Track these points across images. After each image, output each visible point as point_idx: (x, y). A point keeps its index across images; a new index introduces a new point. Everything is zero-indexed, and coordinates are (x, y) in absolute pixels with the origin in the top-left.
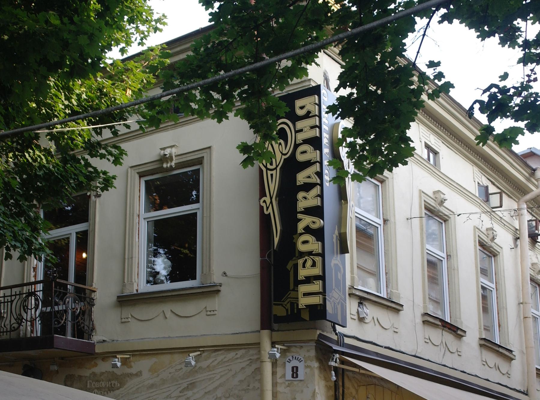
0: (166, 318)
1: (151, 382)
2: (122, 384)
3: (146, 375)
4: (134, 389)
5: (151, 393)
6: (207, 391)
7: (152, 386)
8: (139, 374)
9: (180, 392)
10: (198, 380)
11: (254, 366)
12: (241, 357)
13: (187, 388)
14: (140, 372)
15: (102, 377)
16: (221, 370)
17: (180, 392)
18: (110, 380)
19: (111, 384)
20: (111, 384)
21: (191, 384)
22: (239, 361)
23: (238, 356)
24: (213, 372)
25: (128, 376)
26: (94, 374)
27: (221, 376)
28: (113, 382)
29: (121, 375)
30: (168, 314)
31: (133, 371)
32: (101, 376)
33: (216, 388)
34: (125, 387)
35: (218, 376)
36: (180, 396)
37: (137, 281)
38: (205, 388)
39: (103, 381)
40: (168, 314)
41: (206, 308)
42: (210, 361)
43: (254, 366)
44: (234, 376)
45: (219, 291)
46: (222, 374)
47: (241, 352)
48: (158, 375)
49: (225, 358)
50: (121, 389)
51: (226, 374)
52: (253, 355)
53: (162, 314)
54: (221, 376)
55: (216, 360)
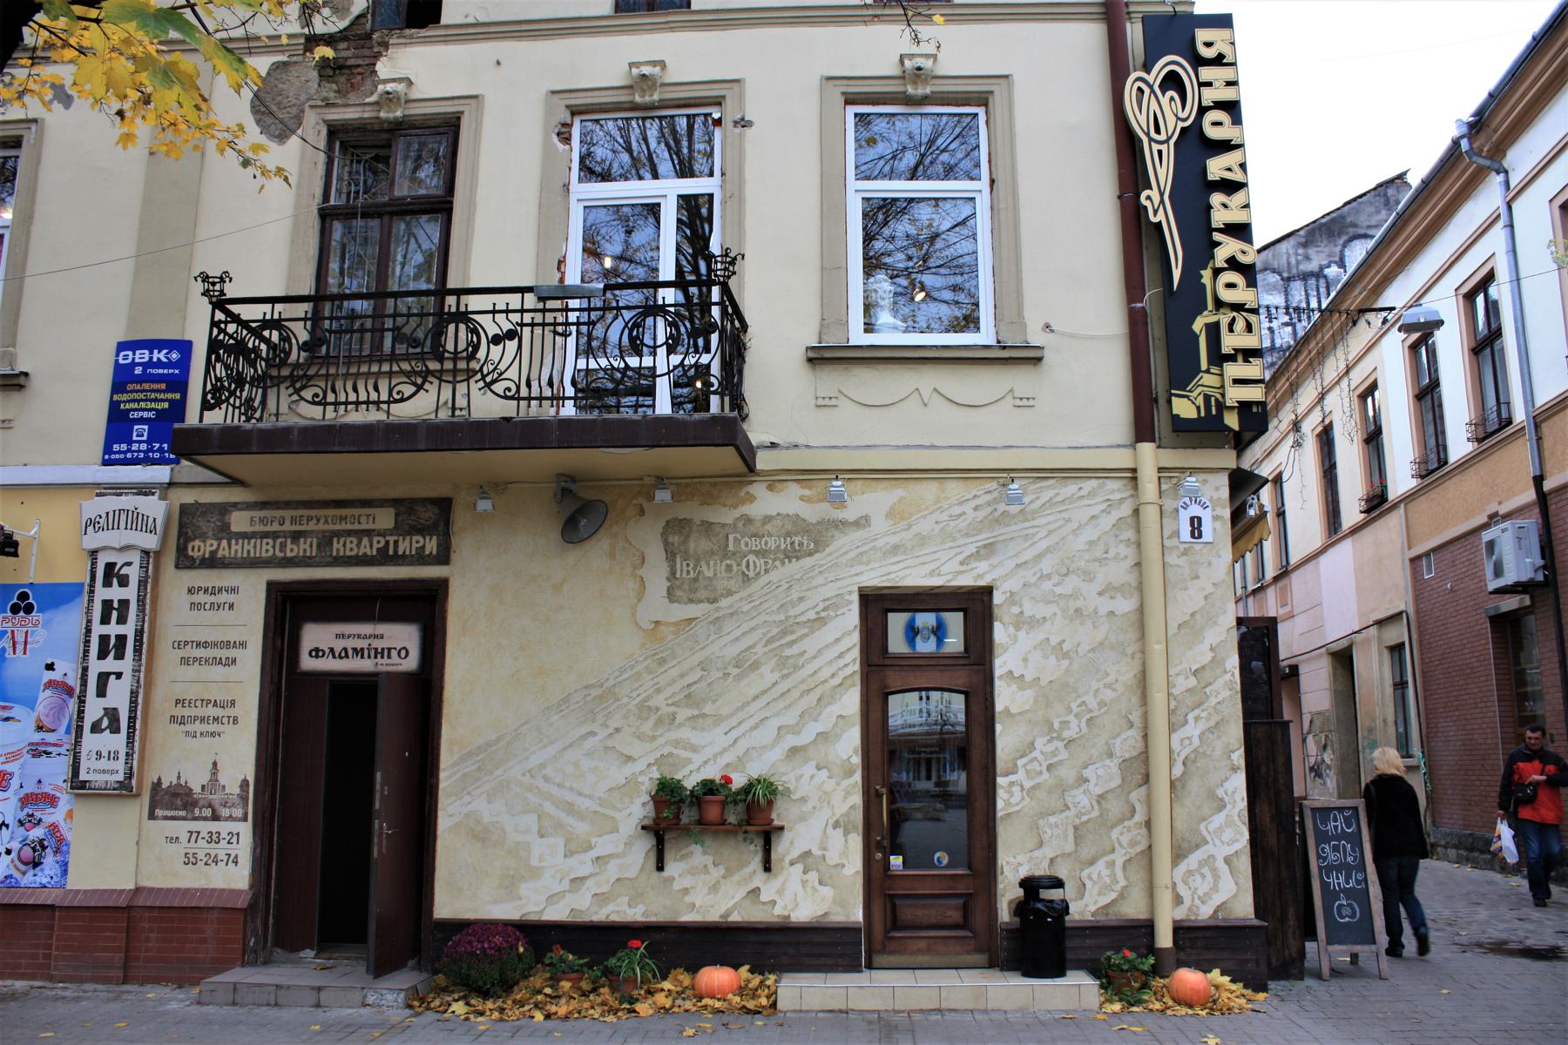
1: (893, 540)
2: (819, 545)
3: (879, 524)
4: (852, 555)
5: (893, 564)
7: (895, 549)
9: (962, 563)
12: (1091, 494)
13: (977, 556)
15: (768, 527)
17: (962, 563)
18: (788, 534)
19: (792, 543)
20: (792, 543)
21: (985, 546)
22: (1086, 502)
25: (837, 527)
26: (748, 520)
27: (1050, 532)
28: (797, 539)
29: (819, 523)
31: (850, 514)
33: (1040, 556)
34: (828, 550)
35: (1043, 533)
38: (1016, 555)
39: (770, 535)
41: (1011, 390)
45: (1039, 359)
46: (1051, 527)
48: (910, 526)
49: (1057, 494)
50: (817, 555)
51: (1060, 527)
52: (1113, 491)
55: (1038, 498)
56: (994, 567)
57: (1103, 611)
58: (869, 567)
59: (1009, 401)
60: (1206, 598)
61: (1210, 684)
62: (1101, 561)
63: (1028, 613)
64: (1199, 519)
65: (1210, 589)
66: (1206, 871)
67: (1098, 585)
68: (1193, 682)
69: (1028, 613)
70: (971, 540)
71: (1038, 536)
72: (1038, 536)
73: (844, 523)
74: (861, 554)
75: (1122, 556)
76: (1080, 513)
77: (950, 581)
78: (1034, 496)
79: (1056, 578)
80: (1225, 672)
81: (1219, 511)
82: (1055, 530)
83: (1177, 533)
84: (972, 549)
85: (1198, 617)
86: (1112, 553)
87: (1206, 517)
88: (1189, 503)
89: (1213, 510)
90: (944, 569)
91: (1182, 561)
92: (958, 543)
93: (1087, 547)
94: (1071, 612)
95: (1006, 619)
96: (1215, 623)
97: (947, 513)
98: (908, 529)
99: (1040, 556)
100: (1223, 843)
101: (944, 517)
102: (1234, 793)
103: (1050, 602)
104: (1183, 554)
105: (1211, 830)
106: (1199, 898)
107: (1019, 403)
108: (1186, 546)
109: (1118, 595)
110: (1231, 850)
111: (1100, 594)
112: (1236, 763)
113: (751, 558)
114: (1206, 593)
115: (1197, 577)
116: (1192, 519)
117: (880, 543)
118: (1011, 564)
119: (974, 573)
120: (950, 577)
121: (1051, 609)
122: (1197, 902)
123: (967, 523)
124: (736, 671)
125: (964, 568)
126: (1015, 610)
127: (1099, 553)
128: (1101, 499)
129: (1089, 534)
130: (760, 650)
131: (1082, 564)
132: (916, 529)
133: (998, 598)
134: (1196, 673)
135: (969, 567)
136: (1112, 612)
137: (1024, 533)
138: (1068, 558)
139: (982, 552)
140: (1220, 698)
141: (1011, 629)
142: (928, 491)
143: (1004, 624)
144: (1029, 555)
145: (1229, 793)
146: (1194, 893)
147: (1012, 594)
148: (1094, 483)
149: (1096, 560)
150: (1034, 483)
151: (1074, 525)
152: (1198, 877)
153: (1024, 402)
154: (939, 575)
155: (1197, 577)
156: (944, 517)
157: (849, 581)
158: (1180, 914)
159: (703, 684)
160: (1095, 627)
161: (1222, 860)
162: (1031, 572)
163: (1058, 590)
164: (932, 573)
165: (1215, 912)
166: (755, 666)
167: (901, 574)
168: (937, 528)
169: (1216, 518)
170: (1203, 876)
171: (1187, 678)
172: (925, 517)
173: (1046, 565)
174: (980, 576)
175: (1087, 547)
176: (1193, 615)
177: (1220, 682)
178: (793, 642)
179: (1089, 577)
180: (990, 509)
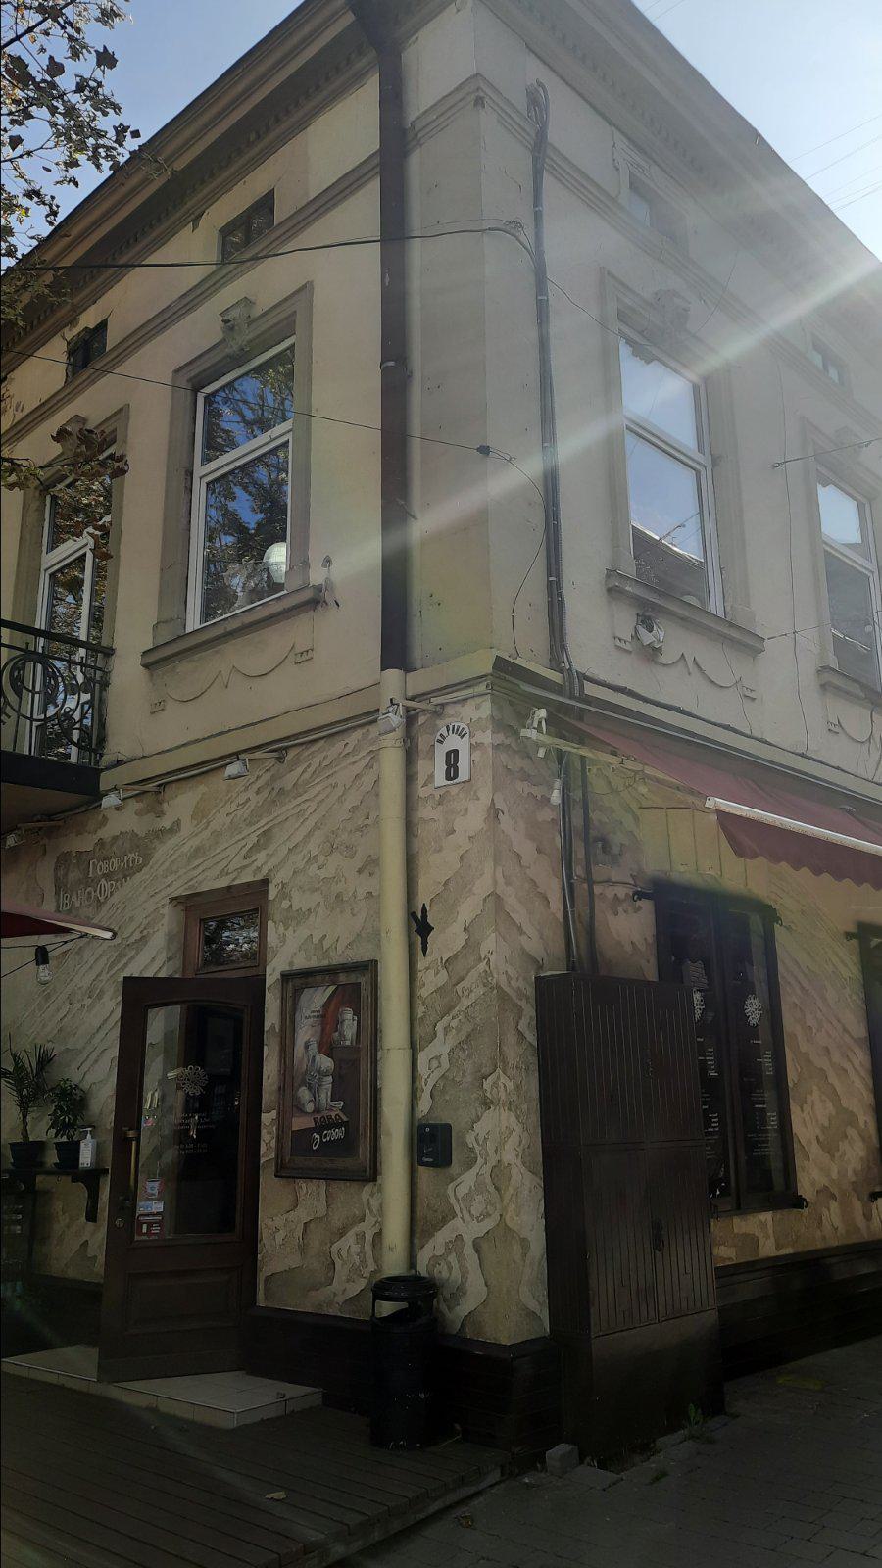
1: (195, 842)
2: (147, 857)
3: (187, 827)
7: (198, 851)
13: (257, 847)
14: (178, 823)
15: (114, 848)
16: (317, 789)
22: (352, 759)
23: (349, 749)
24: (305, 797)
25: (157, 837)
26: (101, 842)
32: (112, 845)
33: (309, 835)
35: (313, 805)
36: (246, 867)
42: (300, 770)
44: (340, 799)
46: (319, 798)
48: (208, 823)
50: (145, 870)
55: (308, 767)
56: (270, 856)
57: (361, 893)
58: (178, 874)
64: (456, 752)
66: (452, 1258)
68: (443, 976)
71: (310, 810)
73: (162, 831)
79: (322, 859)
80: (480, 960)
83: (431, 777)
84: (254, 838)
85: (451, 885)
87: (462, 745)
88: (445, 734)
90: (231, 868)
92: (245, 833)
95: (277, 917)
96: (471, 889)
98: (206, 828)
99: (309, 835)
100: (472, 1216)
108: (442, 791)
110: (480, 1229)
111: (360, 872)
113: (103, 881)
116: (448, 754)
117: (185, 849)
121: (317, 897)
124: (88, 1001)
126: (285, 904)
129: (352, 799)
130: (104, 977)
131: (344, 836)
132: (213, 826)
133: (272, 892)
134: (447, 964)
137: (300, 808)
141: (281, 929)
143: (276, 923)
144: (299, 837)
148: (357, 734)
149: (359, 829)
150: (307, 748)
151: (339, 791)
154: (228, 874)
157: (163, 893)
159: (69, 1017)
160: (353, 915)
161: (471, 1243)
162: (301, 856)
163: (323, 874)
164: (224, 873)
166: (100, 996)
167: (200, 878)
168: (229, 820)
169: (473, 747)
173: (313, 847)
174: (259, 869)
176: (446, 883)
177: (473, 976)
178: (126, 965)
180: (269, 789)
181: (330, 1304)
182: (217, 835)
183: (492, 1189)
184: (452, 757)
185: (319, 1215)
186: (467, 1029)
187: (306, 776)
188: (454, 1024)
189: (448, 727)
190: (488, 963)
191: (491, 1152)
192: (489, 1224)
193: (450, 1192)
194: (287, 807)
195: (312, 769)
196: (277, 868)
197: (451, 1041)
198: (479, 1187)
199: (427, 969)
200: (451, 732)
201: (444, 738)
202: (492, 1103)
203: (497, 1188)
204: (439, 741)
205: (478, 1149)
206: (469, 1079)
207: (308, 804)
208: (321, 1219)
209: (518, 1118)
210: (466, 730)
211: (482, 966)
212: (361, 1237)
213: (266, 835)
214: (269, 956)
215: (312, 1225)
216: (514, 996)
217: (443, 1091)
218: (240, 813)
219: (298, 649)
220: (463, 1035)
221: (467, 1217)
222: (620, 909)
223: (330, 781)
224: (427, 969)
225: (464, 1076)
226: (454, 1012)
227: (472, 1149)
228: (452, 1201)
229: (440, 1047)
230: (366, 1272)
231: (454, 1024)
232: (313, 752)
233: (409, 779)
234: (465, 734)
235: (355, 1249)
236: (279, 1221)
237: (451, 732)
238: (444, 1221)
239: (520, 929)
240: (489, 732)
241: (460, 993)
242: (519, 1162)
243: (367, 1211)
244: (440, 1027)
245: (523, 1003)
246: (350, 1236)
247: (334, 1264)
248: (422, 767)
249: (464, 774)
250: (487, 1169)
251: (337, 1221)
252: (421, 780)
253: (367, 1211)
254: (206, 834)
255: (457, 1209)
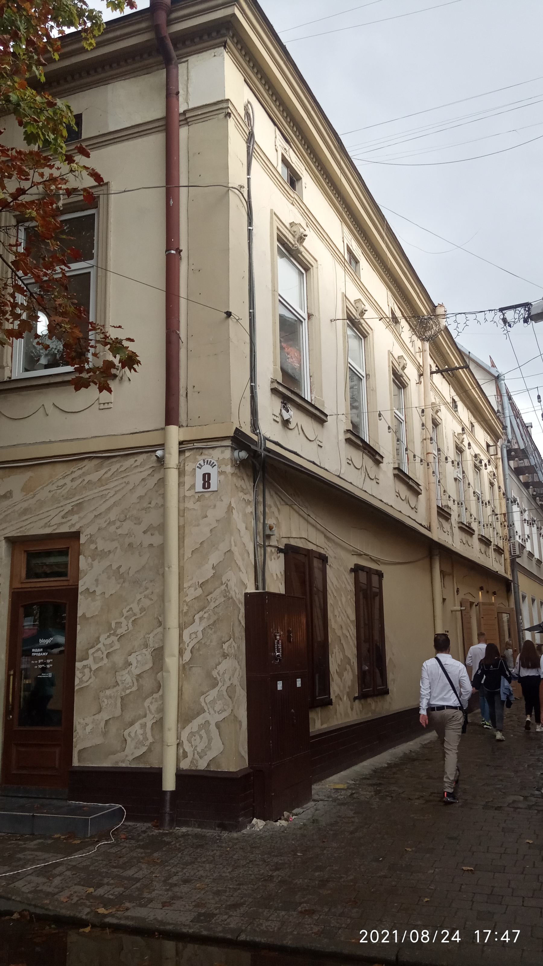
0: (47, 415)
1: (25, 505)
3: (18, 495)
5: (24, 521)
6: (97, 513)
7: (26, 511)
8: (8, 495)
9: (63, 517)
10: (85, 499)
11: (157, 476)
13: (71, 512)
14: (10, 492)
16: (116, 483)
17: (63, 517)
23: (138, 463)
27: (116, 492)
30: (50, 409)
33: (109, 509)
35: (113, 492)
36: (62, 523)
37: (10, 364)
40: (50, 409)
41: (98, 399)
42: (103, 471)
43: (157, 476)
46: (117, 489)
47: (141, 458)
49: (121, 466)
51: (123, 488)
53: (42, 409)
54: (116, 492)
55: (110, 470)
56: (81, 518)
57: (146, 544)
59: (96, 406)
60: (211, 530)
61: (211, 593)
62: (146, 509)
63: (99, 549)
64: (209, 475)
65: (215, 524)
66: (203, 732)
67: (143, 527)
68: (199, 591)
69: (99, 549)
70: (68, 501)
71: (110, 495)
72: (108, 496)
74: (6, 516)
75: (160, 505)
76: (135, 478)
77: (54, 530)
78: (107, 469)
79: (118, 524)
80: (222, 584)
81: (223, 468)
82: (119, 490)
83: (193, 486)
84: (69, 507)
85: (205, 545)
86: (153, 503)
87: (214, 472)
88: (202, 464)
89: (219, 467)
90: (53, 522)
91: (197, 506)
92: (61, 504)
93: (138, 501)
94: (126, 546)
96: (217, 548)
97: (56, 485)
98: (33, 498)
99: (109, 509)
101: (54, 487)
102: (224, 673)
103: (113, 540)
104: (199, 500)
105: (207, 701)
106: (198, 753)
107: (102, 406)
109: (156, 533)
110: (220, 717)
111: (145, 532)
112: (226, 651)
114: (211, 527)
115: (206, 516)
116: (204, 475)
118: (92, 516)
119: (69, 524)
120: (55, 527)
121: (116, 544)
122: (196, 756)
123: (67, 490)
125: (65, 520)
126: (93, 547)
127: (145, 505)
128: (147, 467)
129: (140, 491)
132: (37, 497)
133: (83, 539)
134: (202, 585)
135: (68, 519)
136: (152, 545)
138: (126, 509)
139: (75, 509)
140: (217, 603)
141: (90, 559)
142: (46, 471)
144: (103, 508)
145: (221, 673)
146: (195, 749)
147: (91, 536)
149: (145, 509)
151: (130, 487)
152: (197, 737)
153: (106, 406)
154: (49, 526)
155: (206, 516)
156: (54, 487)
158: (185, 765)
161: (214, 724)
163: (119, 531)
164: (46, 525)
165: (208, 765)
167: (28, 527)
168: (50, 495)
169: (220, 473)
170: (201, 737)
171: (196, 589)
172: (42, 489)
173: (112, 516)
174: (73, 525)
175: (138, 501)
176: (201, 543)
177: (218, 591)
179: (138, 521)
180: (81, 480)
181: (123, 761)
182: (41, 504)
183: (227, 697)
184: (207, 478)
185: (116, 715)
186: (215, 618)
187: (106, 476)
188: (206, 615)
189: (204, 460)
190: (227, 586)
191: (227, 680)
192: (225, 714)
193: (202, 699)
194: (96, 491)
195: (110, 473)
196: (88, 525)
197: (204, 624)
198: (220, 696)
199: (189, 587)
200: (206, 463)
201: (202, 466)
202: (228, 655)
203: (230, 697)
204: (198, 467)
205: (219, 678)
206: (214, 643)
207: (108, 491)
208: (118, 718)
209: (238, 662)
210: (215, 463)
211: (223, 587)
212: (144, 726)
213: (79, 507)
214: (81, 575)
215: (111, 721)
216: (237, 602)
217: (199, 650)
218: (59, 491)
219: (101, 402)
220: (211, 621)
221: (212, 712)
222: (272, 557)
223: (124, 480)
224: (189, 587)
225: (211, 642)
226: (205, 610)
227: (215, 679)
228: (203, 704)
229: (198, 627)
230: (148, 743)
231: (206, 615)
232: (112, 462)
233: (180, 484)
234: (215, 465)
235: (140, 731)
236: (89, 720)
237: (206, 463)
238: (198, 714)
239: (240, 568)
240: (229, 466)
241: (209, 600)
242: (239, 684)
243: (148, 712)
244: (197, 617)
245: (240, 606)
246: (137, 725)
247: (126, 740)
248: (188, 479)
249: (214, 486)
250: (224, 688)
251: (128, 717)
252: (187, 486)
253: (148, 712)
254: (32, 501)
255: (206, 709)
